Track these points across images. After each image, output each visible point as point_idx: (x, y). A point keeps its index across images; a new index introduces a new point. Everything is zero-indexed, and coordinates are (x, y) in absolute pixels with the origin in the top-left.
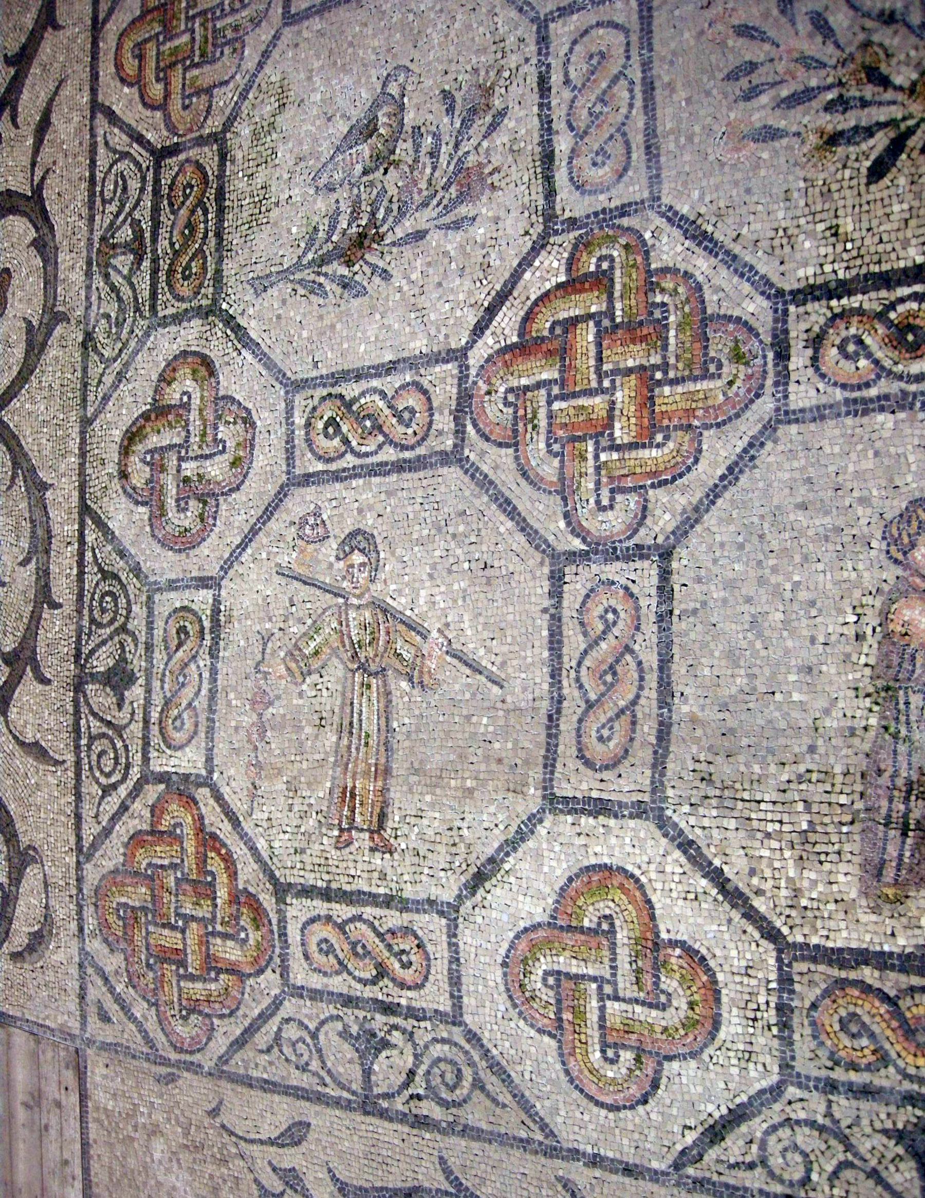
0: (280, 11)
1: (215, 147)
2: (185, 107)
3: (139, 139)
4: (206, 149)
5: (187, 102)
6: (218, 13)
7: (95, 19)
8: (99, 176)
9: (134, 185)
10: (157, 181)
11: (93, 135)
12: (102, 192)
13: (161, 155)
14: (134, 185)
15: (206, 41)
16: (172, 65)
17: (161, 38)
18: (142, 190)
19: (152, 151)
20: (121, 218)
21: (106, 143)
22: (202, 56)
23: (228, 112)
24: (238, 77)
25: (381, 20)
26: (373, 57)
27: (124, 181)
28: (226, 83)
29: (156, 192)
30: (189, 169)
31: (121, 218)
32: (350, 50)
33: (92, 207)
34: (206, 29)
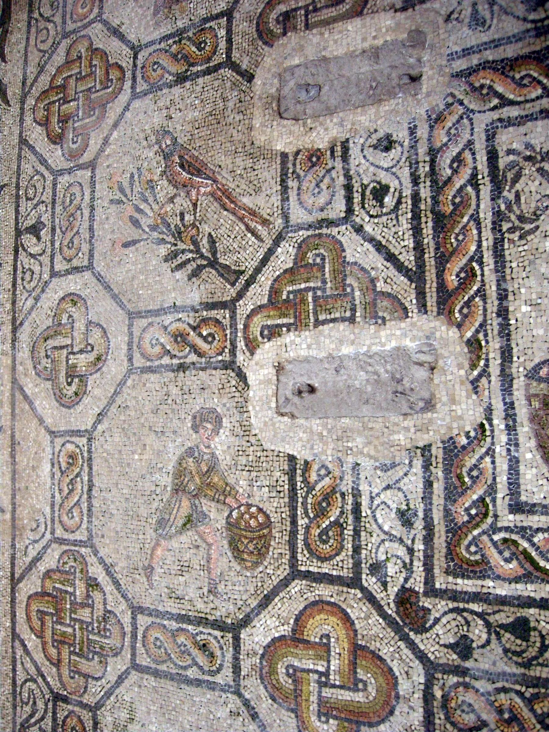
0: (129, 656)
1: (90, 714)
2: (72, 678)
3: (43, 676)
4: (85, 712)
5: (72, 674)
6: (90, 629)
7: (13, 574)
8: (19, 683)
9: (40, 705)
10: (54, 713)
11: (14, 652)
12: (20, 693)
13: (57, 698)
14: (40, 705)
15: (83, 642)
16: (63, 643)
17: (55, 619)
18: (46, 711)
19: (52, 691)
20: (33, 720)
21: (22, 663)
22: (81, 650)
23: (98, 697)
24: (103, 680)
25: (193, 706)
26: (188, 727)
27: (34, 698)
28: (97, 679)
29: (54, 719)
30: (75, 720)
31: (33, 720)
32: (174, 713)
33: (15, 699)
34: (83, 634)
